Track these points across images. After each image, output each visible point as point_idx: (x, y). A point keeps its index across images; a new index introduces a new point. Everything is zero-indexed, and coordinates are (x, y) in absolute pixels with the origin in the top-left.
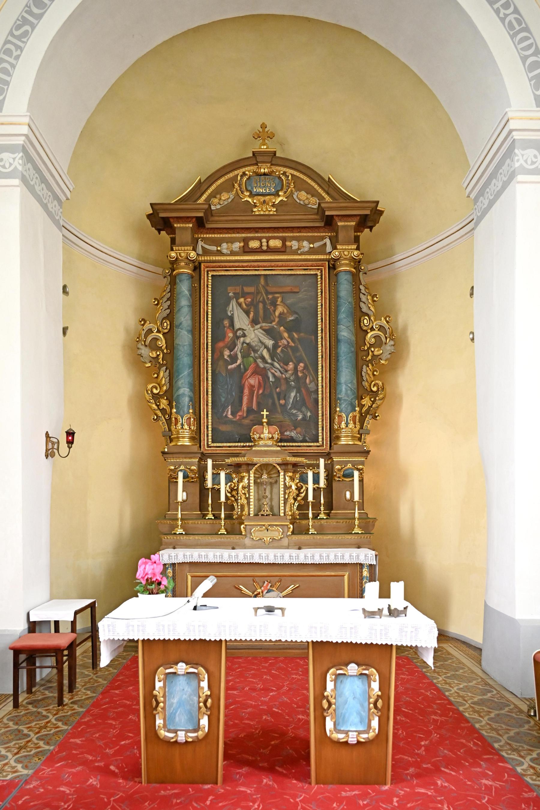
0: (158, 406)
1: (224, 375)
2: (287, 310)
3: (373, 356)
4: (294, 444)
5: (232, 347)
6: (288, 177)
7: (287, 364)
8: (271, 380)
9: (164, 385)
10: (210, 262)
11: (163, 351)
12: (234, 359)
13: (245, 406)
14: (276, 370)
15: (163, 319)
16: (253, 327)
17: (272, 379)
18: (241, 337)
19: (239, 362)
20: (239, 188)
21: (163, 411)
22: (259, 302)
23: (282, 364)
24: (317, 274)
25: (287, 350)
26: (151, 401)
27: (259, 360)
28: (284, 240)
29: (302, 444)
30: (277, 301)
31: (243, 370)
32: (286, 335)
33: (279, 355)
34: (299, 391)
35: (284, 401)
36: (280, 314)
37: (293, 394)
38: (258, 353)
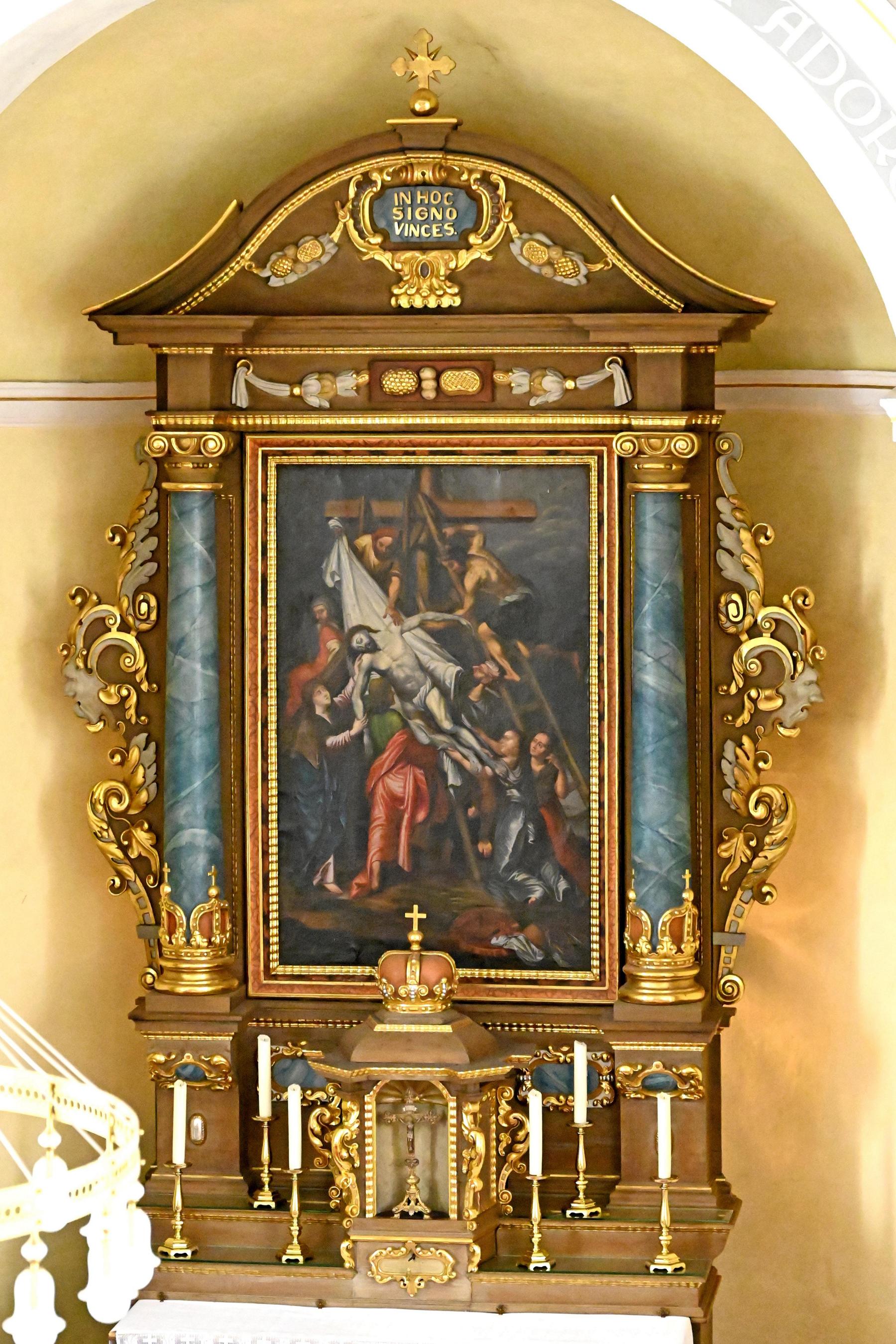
0: (124, 849)
1: (315, 764)
2: (498, 572)
3: (757, 713)
4: (517, 974)
6: (496, 187)
7: (498, 736)
8: (451, 780)
9: (141, 787)
10: (271, 431)
11: (137, 687)
13: (374, 859)
14: (466, 752)
15: (137, 592)
16: (397, 621)
17: (454, 777)
18: (363, 652)
19: (357, 726)
20: (351, 222)
21: (140, 865)
22: (417, 546)
23: (483, 737)
24: (587, 467)
25: (498, 691)
26: (105, 834)
27: (418, 721)
29: (542, 974)
30: (469, 545)
31: (368, 751)
32: (495, 648)
33: (476, 708)
34: (534, 817)
35: (489, 846)
36: (481, 584)
37: (515, 826)
38: (415, 700)
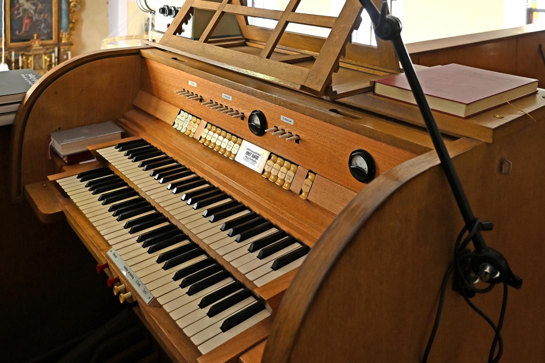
5: (18, 9)
12: (19, 14)
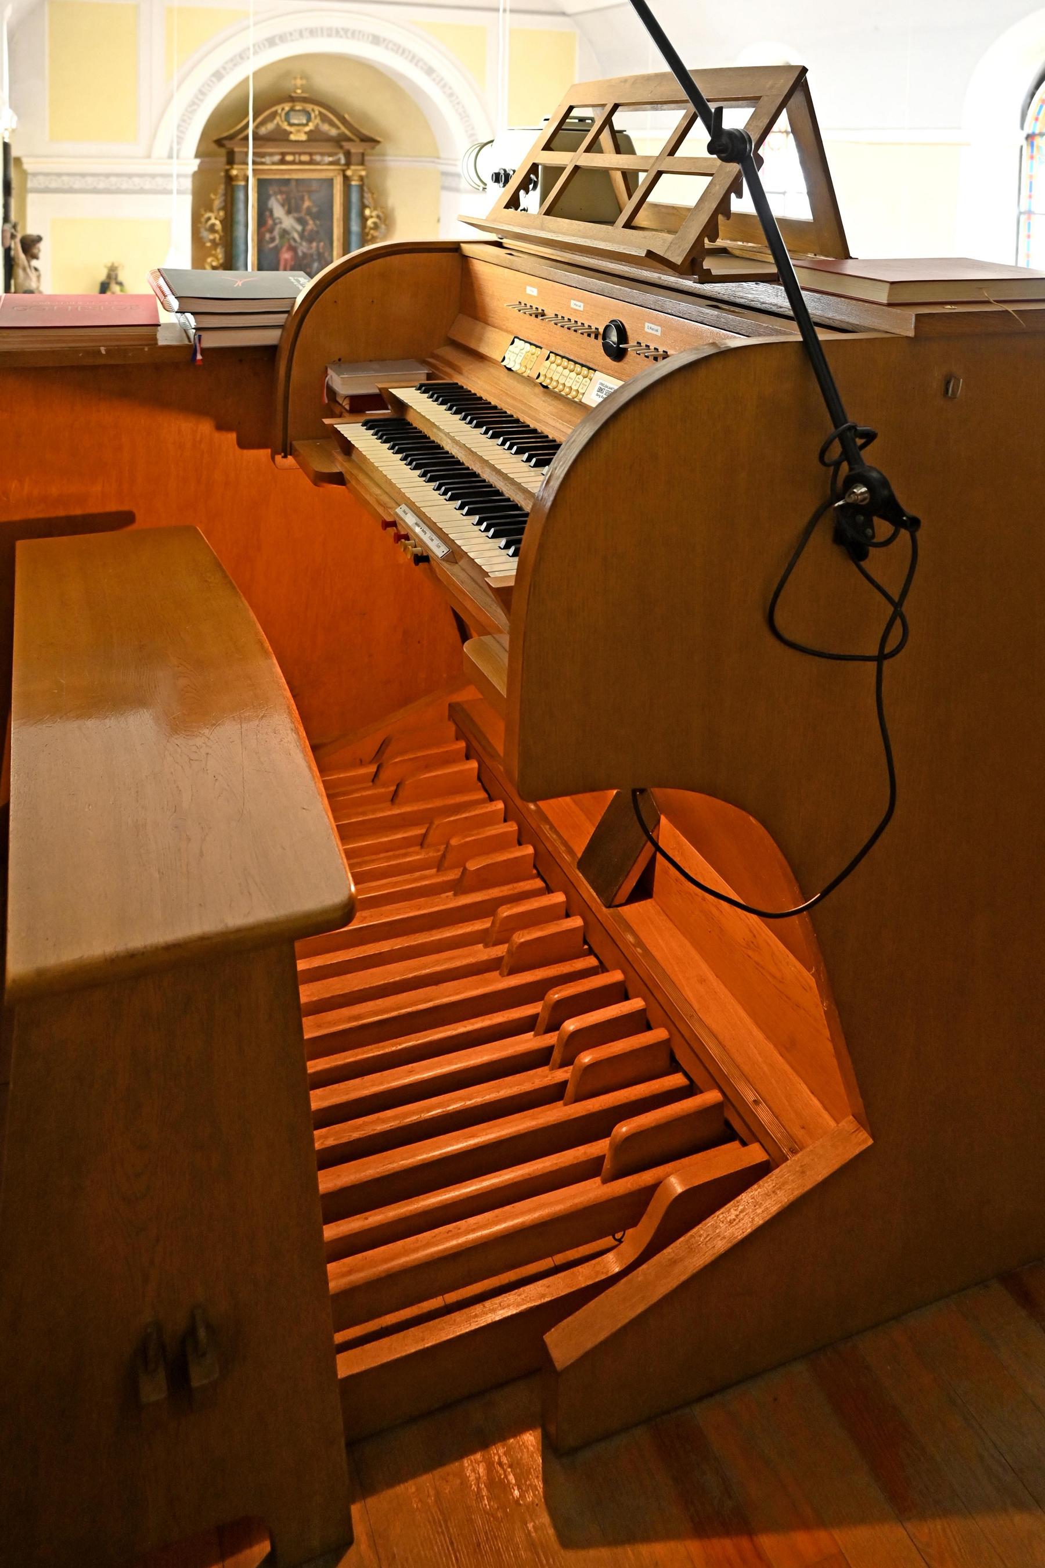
5: (271, 231)
12: (273, 239)
28: (311, 154)
